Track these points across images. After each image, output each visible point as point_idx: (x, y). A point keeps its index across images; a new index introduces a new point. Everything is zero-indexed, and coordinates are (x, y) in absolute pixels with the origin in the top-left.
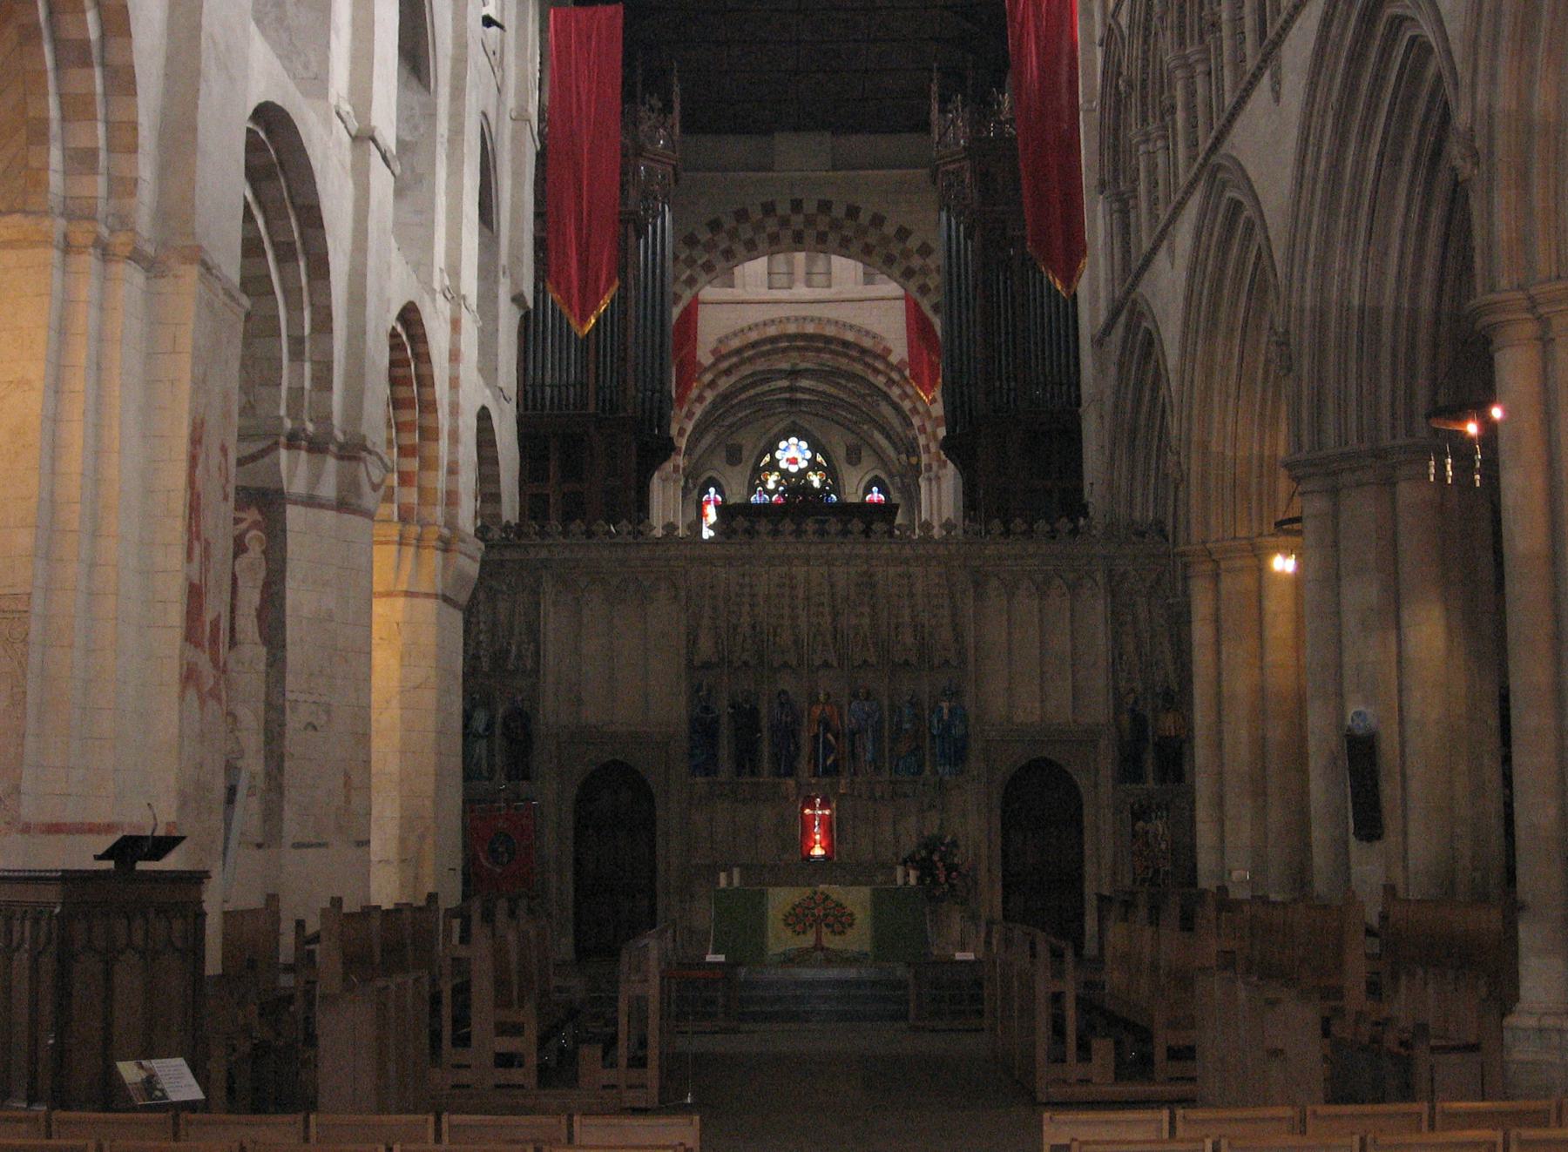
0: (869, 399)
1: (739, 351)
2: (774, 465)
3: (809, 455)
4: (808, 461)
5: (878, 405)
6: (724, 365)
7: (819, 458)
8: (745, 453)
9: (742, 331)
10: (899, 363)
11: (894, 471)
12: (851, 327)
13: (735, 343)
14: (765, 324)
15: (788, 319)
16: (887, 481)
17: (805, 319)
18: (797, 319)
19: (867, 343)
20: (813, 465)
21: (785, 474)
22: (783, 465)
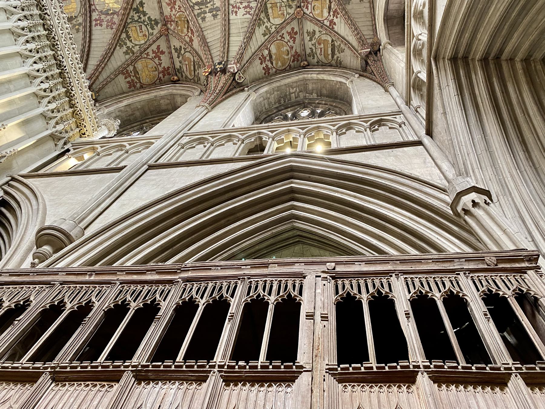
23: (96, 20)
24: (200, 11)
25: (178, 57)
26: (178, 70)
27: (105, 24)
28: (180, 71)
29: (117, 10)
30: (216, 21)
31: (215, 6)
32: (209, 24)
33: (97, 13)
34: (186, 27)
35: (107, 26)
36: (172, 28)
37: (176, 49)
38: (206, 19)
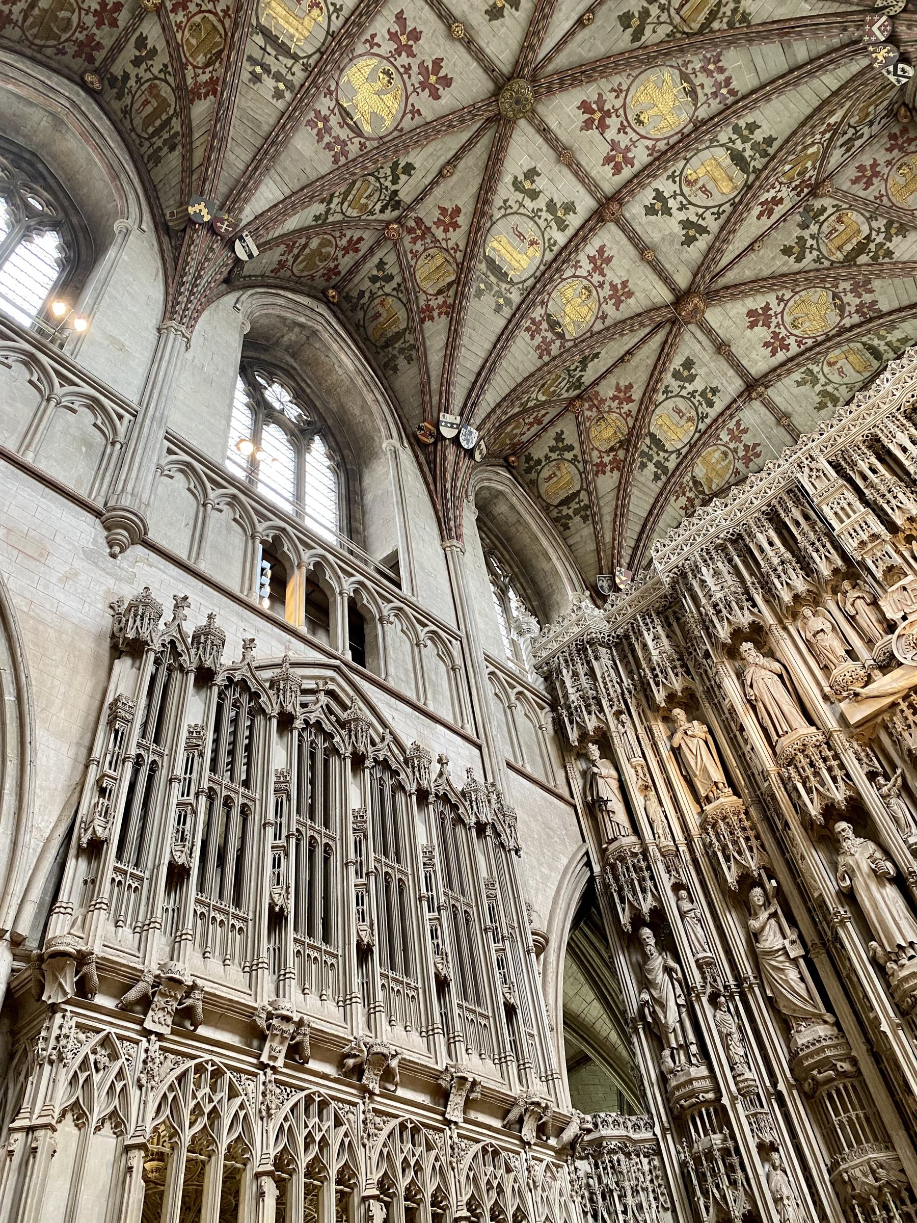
0: (863, 259)
5: (889, 254)
23: (533, 321)
24: (646, 450)
25: (552, 450)
26: (529, 458)
27: (538, 339)
28: (532, 463)
29: (567, 337)
30: (653, 486)
31: (666, 464)
32: (643, 479)
33: (543, 312)
34: (612, 444)
35: (538, 347)
36: (588, 413)
37: (559, 437)
38: (645, 470)
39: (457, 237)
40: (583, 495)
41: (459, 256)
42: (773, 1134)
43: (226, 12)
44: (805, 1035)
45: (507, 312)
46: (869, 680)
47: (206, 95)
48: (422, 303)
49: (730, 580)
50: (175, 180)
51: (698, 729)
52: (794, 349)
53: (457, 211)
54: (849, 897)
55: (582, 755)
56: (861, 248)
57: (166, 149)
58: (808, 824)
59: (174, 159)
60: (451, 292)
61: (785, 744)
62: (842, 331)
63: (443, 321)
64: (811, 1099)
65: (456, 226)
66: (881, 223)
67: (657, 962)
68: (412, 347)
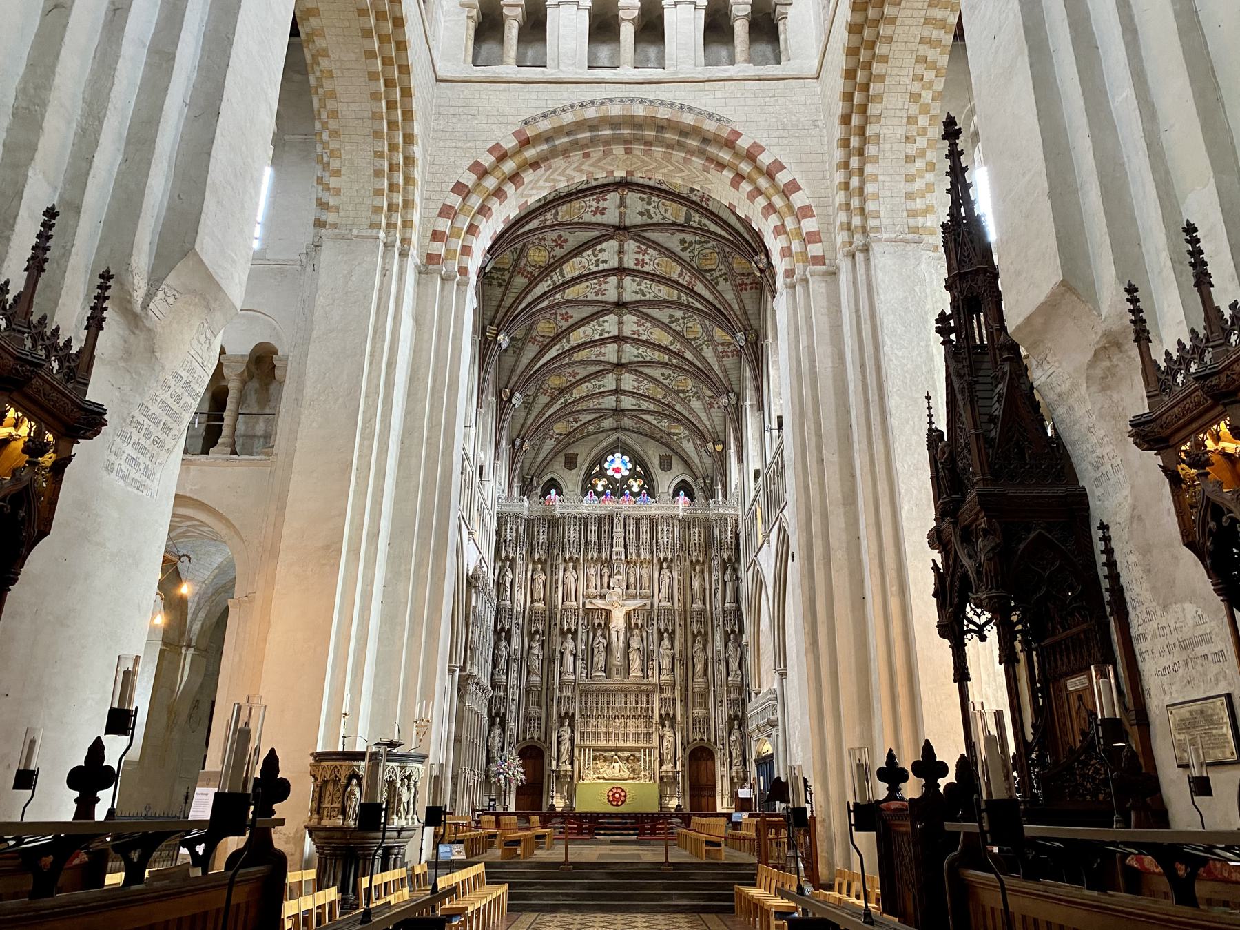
0: (682, 395)
1: (547, 137)
2: (602, 474)
3: (630, 466)
4: (630, 470)
5: (690, 401)
6: (530, 153)
7: (638, 469)
8: (580, 460)
9: (554, 112)
10: (752, 146)
11: (698, 474)
12: (690, 109)
13: (545, 125)
14: (582, 106)
15: (611, 100)
16: (692, 484)
17: (632, 100)
18: (622, 101)
19: (710, 126)
20: (634, 474)
21: (611, 480)
22: (610, 473)
39: (565, 325)
40: (531, 398)
41: (560, 331)
42: (516, 697)
43: (554, 257)
44: (534, 678)
45: (560, 351)
46: (595, 597)
47: (526, 277)
48: (534, 335)
49: (578, 535)
50: (495, 303)
51: (543, 577)
52: (641, 392)
53: (572, 317)
54: (562, 653)
55: (504, 562)
56: (684, 392)
57: (495, 282)
58: (562, 630)
59: (499, 291)
60: (548, 340)
61: (567, 604)
62: (659, 401)
63: (537, 348)
64: (528, 692)
65: (567, 320)
66: (695, 390)
67: (504, 643)
68: (518, 348)
